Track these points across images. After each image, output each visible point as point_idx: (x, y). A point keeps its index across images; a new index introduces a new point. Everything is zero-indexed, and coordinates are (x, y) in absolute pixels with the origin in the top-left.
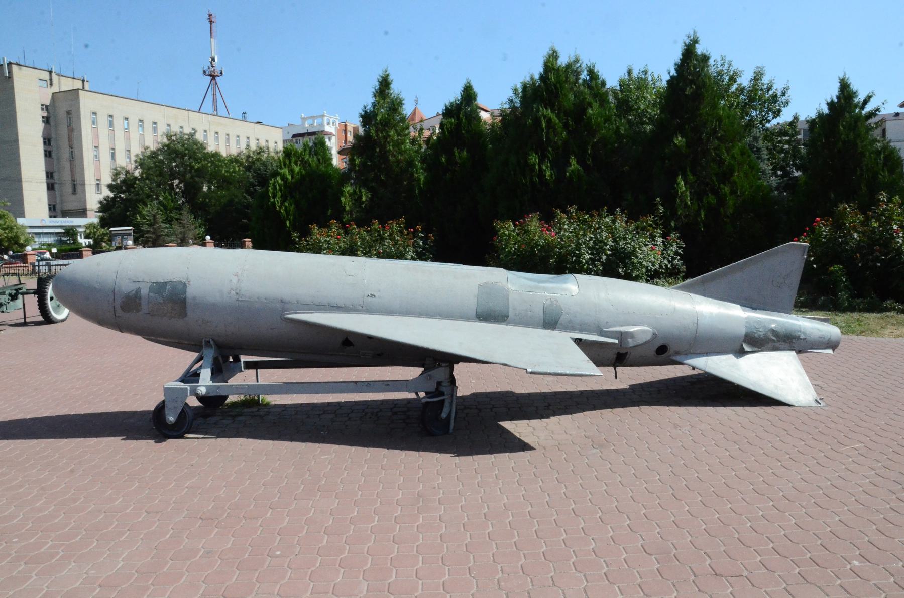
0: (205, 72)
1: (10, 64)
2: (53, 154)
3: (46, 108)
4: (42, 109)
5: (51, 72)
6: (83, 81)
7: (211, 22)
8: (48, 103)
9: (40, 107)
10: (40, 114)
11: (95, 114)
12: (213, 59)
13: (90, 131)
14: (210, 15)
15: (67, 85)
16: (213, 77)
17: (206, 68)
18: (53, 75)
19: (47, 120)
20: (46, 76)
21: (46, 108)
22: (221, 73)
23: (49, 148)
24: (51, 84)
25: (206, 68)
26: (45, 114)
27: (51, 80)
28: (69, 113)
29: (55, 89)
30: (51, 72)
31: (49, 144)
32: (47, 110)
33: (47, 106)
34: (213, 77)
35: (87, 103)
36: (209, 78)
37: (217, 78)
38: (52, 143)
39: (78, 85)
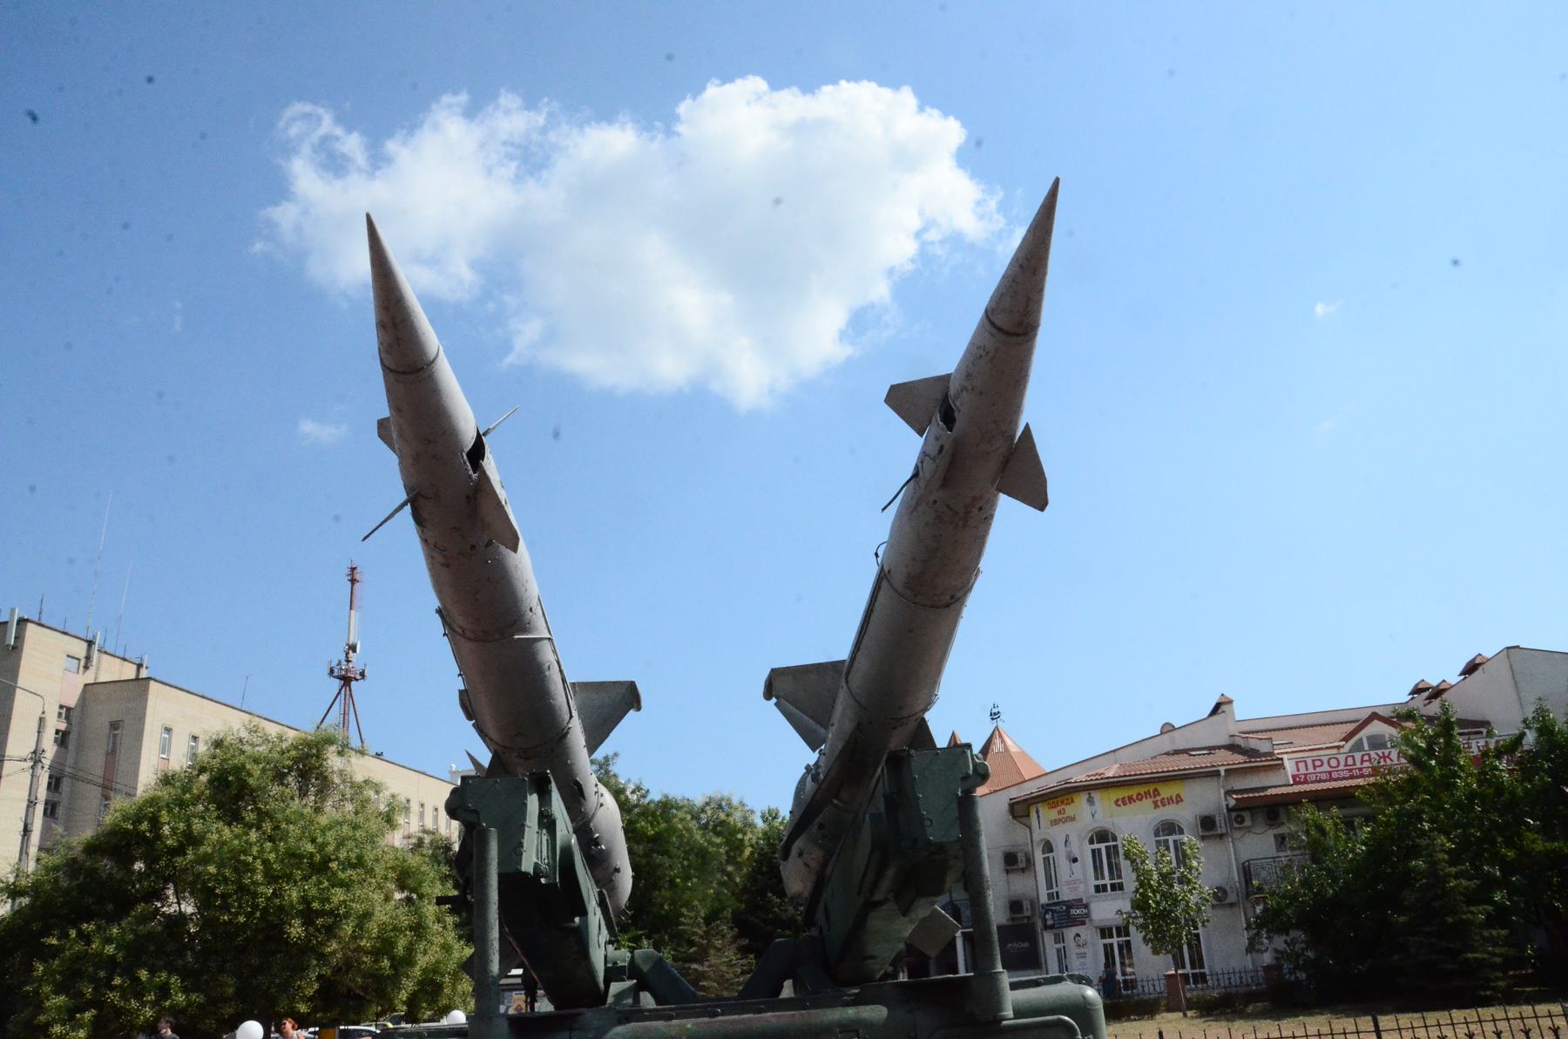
0: (332, 671)
2: (60, 811)
3: (67, 712)
4: (60, 715)
5: (90, 643)
6: (140, 666)
7: (353, 581)
8: (72, 703)
9: (57, 710)
11: (168, 730)
12: (353, 648)
14: (353, 569)
15: (111, 670)
16: (346, 680)
17: (334, 664)
18: (96, 647)
19: (62, 738)
20: (80, 649)
21: (67, 712)
22: (363, 674)
24: (86, 667)
25: (334, 664)
26: (63, 726)
27: (88, 658)
28: (114, 726)
29: (89, 677)
30: (90, 643)
32: (67, 718)
33: (69, 709)
34: (346, 680)
36: (337, 683)
37: (353, 683)
38: (66, 785)
39: (129, 672)
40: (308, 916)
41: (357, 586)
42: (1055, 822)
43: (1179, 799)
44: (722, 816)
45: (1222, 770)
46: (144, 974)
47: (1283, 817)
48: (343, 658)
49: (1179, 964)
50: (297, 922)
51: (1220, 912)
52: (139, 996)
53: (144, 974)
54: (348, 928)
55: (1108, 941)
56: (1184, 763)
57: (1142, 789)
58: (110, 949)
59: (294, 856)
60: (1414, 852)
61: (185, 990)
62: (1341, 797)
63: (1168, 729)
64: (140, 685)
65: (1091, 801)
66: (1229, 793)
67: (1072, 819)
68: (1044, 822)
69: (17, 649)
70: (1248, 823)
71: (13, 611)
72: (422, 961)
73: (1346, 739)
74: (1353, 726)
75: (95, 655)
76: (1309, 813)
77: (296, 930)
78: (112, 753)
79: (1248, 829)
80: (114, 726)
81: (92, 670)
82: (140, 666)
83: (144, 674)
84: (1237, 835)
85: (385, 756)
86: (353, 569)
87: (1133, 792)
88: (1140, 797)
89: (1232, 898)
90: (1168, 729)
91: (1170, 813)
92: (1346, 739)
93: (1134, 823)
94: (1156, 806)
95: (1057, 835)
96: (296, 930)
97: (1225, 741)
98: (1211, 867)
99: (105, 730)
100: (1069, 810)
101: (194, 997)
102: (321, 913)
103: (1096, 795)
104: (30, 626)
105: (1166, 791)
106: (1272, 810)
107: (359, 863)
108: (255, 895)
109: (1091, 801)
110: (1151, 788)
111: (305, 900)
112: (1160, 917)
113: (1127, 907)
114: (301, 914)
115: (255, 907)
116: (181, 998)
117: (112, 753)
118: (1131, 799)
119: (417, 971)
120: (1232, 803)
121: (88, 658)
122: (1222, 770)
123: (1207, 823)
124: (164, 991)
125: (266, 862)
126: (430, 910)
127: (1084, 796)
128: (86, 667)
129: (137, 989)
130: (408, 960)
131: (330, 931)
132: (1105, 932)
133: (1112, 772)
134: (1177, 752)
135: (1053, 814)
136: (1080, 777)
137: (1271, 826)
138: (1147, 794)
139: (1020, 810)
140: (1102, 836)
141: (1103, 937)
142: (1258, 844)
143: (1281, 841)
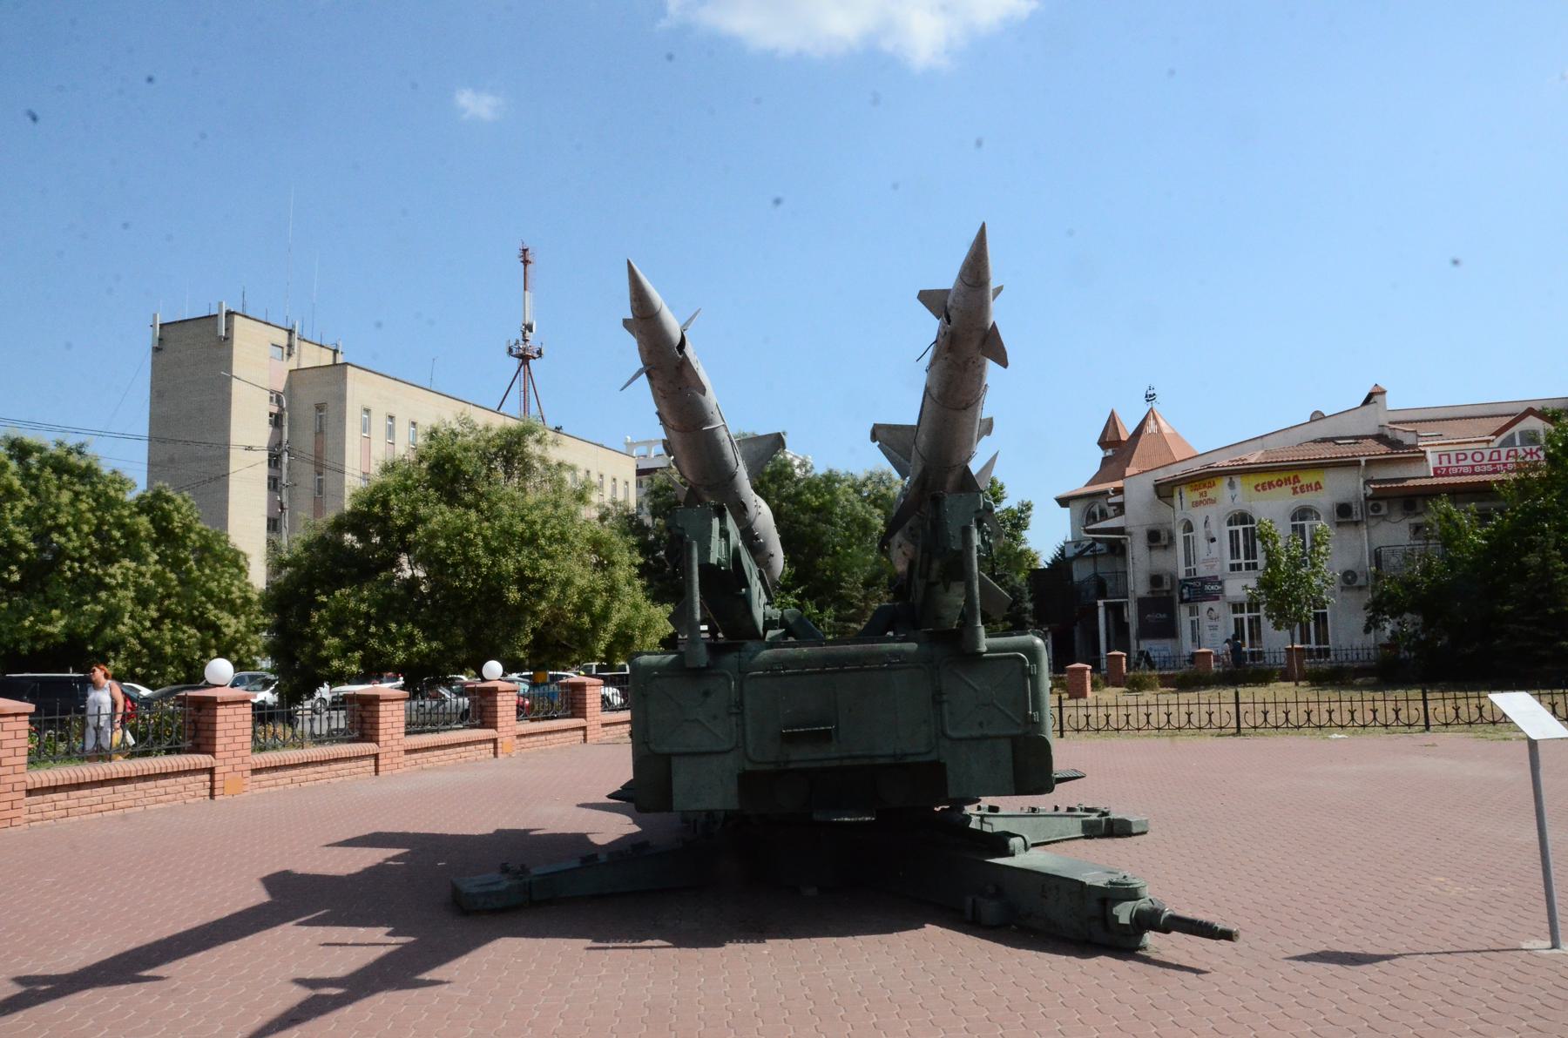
0: (510, 350)
1: (230, 314)
5: (291, 332)
6: (336, 352)
7: (526, 262)
8: (280, 387)
10: (267, 407)
11: (367, 411)
12: (529, 328)
13: (357, 442)
14: (525, 251)
15: (312, 357)
16: (525, 359)
18: (296, 336)
19: (276, 421)
20: (282, 337)
22: (540, 353)
23: (275, 473)
24: (289, 355)
26: (275, 410)
27: (290, 346)
28: (320, 408)
29: (293, 364)
30: (291, 332)
31: (276, 464)
34: (525, 359)
35: (360, 390)
36: (516, 362)
39: (327, 358)
40: (522, 581)
41: (529, 266)
42: (1196, 504)
43: (1318, 486)
44: (883, 489)
45: (1363, 460)
46: (393, 626)
47: (1420, 509)
48: (520, 337)
49: (1305, 639)
50: (514, 588)
51: (1347, 594)
52: (393, 643)
53: (393, 626)
54: (554, 593)
55: (1239, 615)
56: (1327, 452)
57: (1282, 476)
58: (364, 607)
59: (507, 533)
60: (1530, 547)
61: (427, 639)
62: (1480, 492)
63: (1317, 417)
64: (338, 370)
65: (1232, 485)
66: (1367, 482)
67: (1213, 501)
68: (1186, 504)
69: (228, 339)
70: (1384, 511)
71: (220, 304)
72: (616, 618)
73: (1497, 434)
74: (1507, 420)
75: (296, 342)
76: (1444, 505)
77: (513, 595)
78: (320, 432)
79: (1384, 518)
80: (320, 408)
81: (294, 357)
82: (336, 352)
83: (340, 360)
84: (1372, 522)
85: (564, 430)
86: (525, 251)
87: (1274, 478)
88: (1280, 483)
89: (1361, 581)
90: (1317, 417)
91: (1307, 499)
92: (1497, 434)
93: (1272, 508)
94: (1295, 492)
95: (1197, 516)
96: (513, 595)
97: (1373, 430)
98: (1342, 553)
99: (312, 412)
100: (1211, 493)
101: (434, 645)
102: (532, 580)
103: (1237, 480)
104: (237, 318)
105: (1307, 478)
106: (1411, 500)
107: (563, 539)
108: (479, 566)
109: (1232, 485)
110: (1291, 475)
111: (520, 571)
112: (1282, 595)
113: (1253, 583)
114: (515, 582)
115: (479, 575)
116: (423, 646)
117: (320, 432)
118: (1270, 485)
119: (611, 627)
120: (1370, 492)
121: (290, 346)
122: (1363, 460)
123: (1343, 510)
124: (411, 640)
125: (485, 538)
126: (621, 574)
127: (1226, 480)
128: (289, 355)
129: (390, 639)
130: (605, 615)
131: (540, 594)
132: (1237, 607)
133: (1254, 457)
134: (1324, 440)
135: (1195, 496)
136: (1223, 462)
137: (1407, 515)
138: (1287, 481)
139: (1165, 491)
140: (1243, 518)
141: (1235, 611)
142: (1394, 533)
143: (1417, 529)
